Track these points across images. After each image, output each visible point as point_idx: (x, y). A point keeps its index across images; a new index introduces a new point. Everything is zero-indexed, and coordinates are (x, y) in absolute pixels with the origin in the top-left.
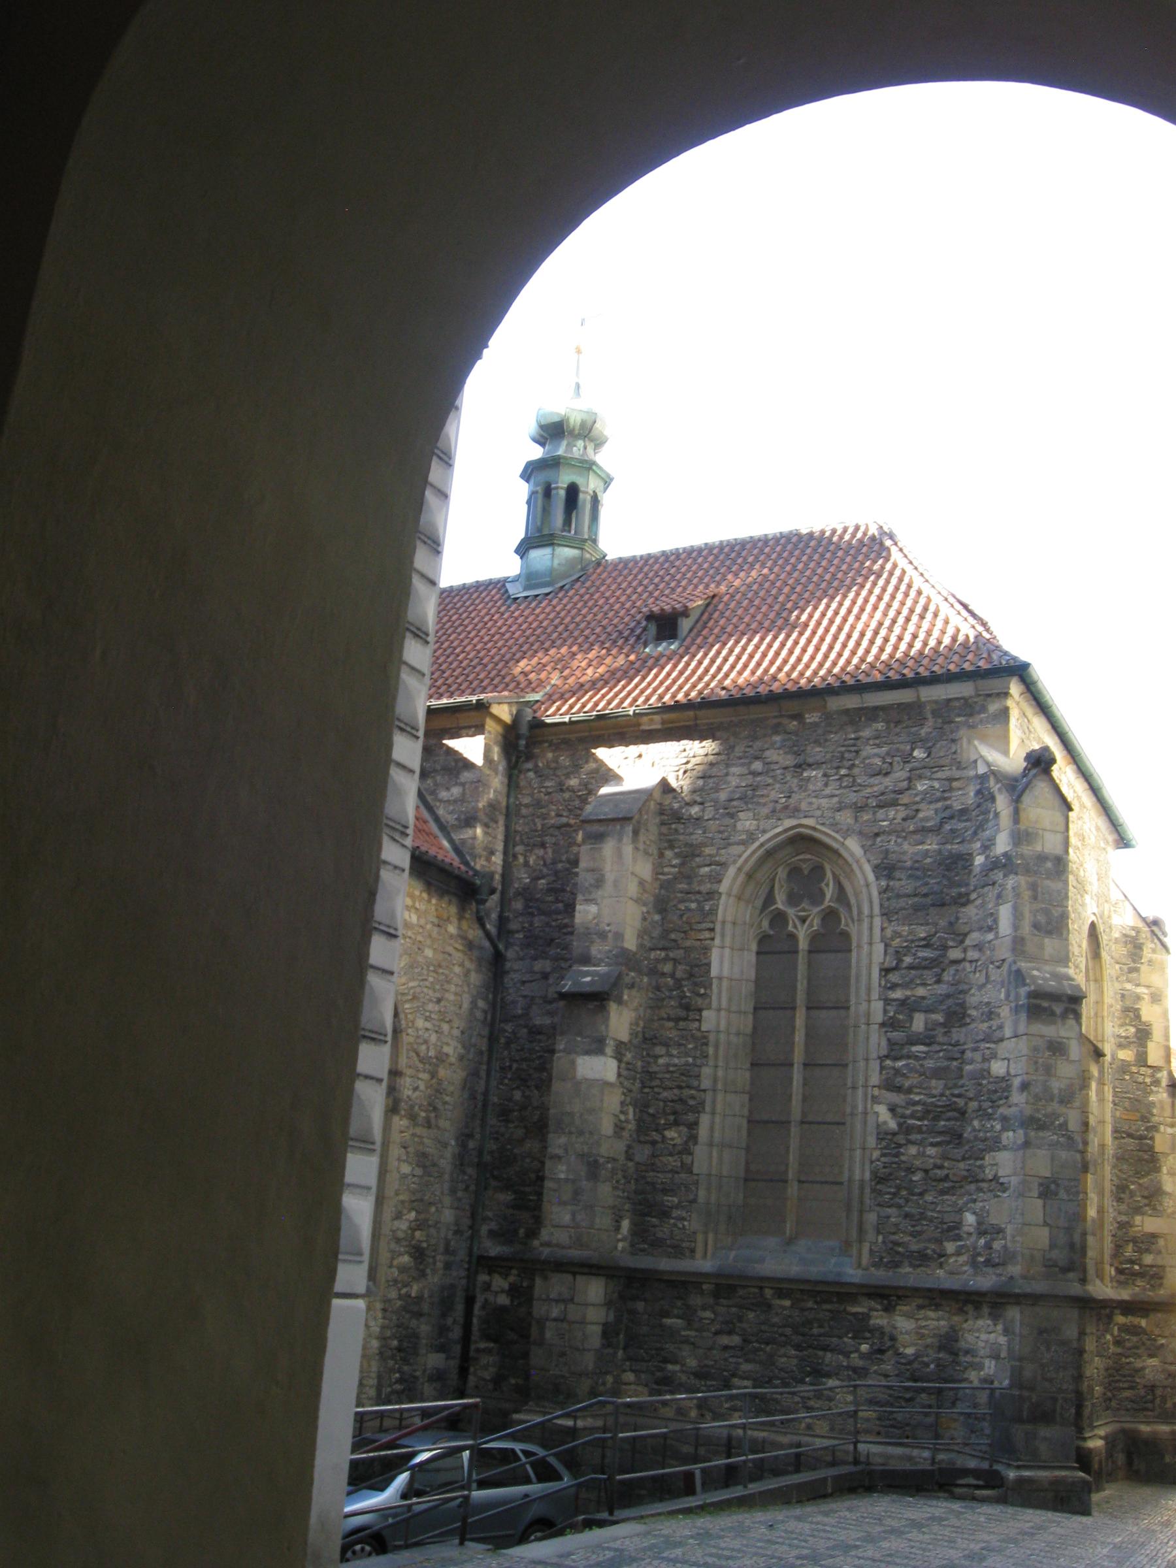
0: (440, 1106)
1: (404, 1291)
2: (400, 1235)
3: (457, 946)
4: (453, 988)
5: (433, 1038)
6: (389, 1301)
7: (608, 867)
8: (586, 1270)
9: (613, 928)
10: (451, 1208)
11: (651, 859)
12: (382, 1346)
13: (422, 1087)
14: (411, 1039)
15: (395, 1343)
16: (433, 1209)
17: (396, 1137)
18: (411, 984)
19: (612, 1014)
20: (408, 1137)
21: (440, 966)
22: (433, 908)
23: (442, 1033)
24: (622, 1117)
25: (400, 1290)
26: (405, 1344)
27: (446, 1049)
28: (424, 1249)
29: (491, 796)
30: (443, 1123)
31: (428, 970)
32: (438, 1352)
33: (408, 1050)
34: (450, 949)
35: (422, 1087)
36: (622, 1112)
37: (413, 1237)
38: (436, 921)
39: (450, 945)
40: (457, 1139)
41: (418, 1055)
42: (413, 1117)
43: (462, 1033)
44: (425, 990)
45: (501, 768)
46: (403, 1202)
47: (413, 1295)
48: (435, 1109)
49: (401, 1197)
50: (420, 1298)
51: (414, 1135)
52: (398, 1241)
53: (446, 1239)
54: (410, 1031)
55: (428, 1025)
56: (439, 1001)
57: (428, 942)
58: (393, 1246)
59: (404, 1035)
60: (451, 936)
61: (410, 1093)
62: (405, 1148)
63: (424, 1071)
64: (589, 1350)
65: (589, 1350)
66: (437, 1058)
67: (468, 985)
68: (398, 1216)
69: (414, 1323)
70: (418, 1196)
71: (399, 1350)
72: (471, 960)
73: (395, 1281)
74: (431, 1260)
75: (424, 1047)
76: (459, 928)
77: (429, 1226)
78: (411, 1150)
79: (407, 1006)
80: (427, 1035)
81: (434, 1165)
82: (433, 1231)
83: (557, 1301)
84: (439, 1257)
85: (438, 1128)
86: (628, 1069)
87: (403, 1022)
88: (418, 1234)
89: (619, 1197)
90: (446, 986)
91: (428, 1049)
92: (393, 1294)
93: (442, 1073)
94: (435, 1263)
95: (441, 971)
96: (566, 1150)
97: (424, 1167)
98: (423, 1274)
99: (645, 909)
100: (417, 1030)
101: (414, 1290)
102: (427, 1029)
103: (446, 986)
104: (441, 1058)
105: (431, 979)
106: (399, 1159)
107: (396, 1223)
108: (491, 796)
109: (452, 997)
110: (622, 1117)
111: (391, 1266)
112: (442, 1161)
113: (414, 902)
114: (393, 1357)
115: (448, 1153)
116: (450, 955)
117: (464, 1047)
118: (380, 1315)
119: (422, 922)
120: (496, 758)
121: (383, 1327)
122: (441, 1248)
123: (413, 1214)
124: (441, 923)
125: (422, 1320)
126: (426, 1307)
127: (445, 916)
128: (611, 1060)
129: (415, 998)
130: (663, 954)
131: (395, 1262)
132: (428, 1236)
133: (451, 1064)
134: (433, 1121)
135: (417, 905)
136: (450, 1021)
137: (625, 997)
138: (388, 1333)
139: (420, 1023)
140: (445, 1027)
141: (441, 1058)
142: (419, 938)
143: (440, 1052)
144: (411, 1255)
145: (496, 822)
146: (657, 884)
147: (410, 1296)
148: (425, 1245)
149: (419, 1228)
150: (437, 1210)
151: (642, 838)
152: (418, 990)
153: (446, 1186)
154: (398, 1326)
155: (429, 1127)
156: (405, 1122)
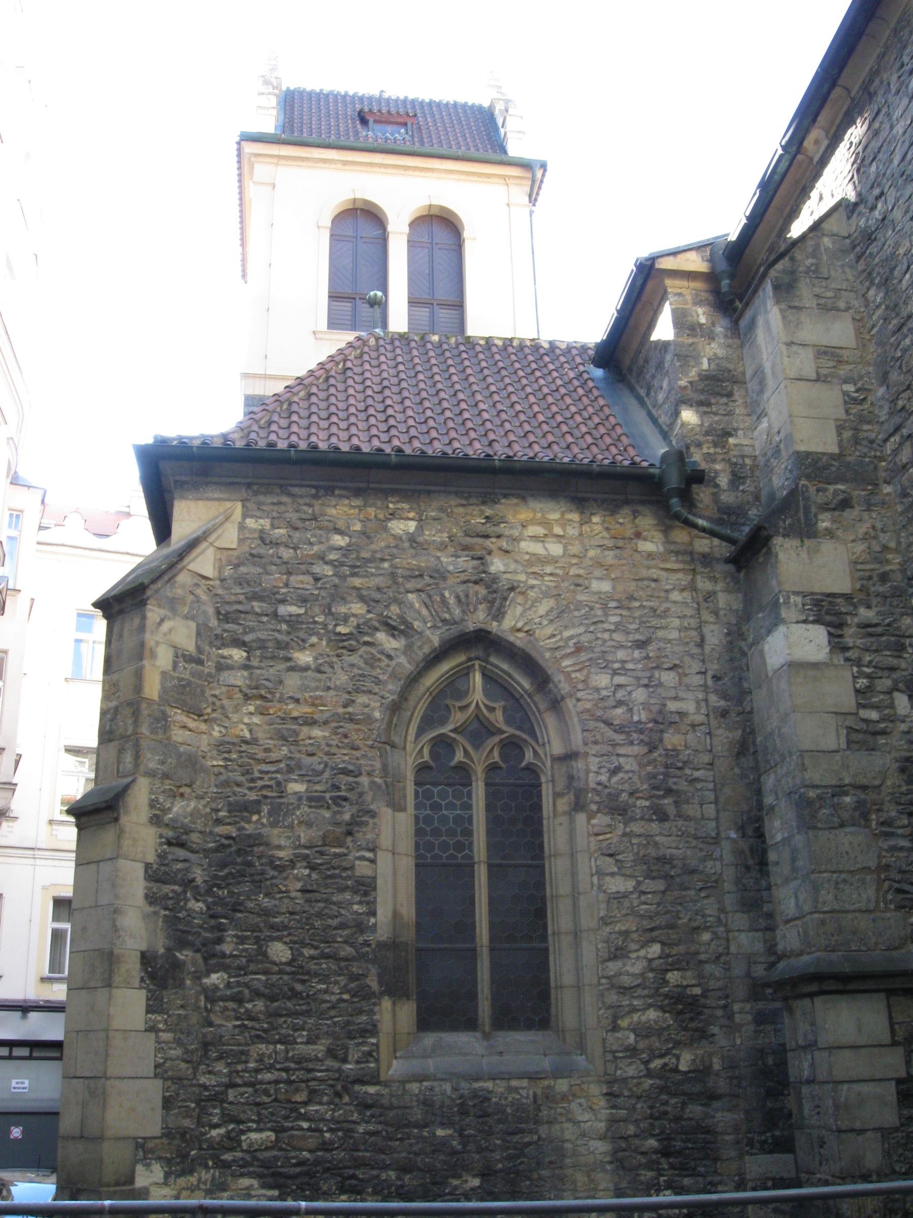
0: (683, 785)
1: (657, 1063)
2: (626, 981)
3: (669, 566)
4: (676, 622)
5: (640, 695)
6: (624, 1080)
7: (765, 356)
8: (814, 987)
9: (782, 434)
10: (752, 929)
11: (847, 316)
12: (615, 1152)
13: (629, 764)
14: (588, 705)
15: (652, 1143)
16: (706, 936)
17: (581, 841)
18: (567, 634)
19: (781, 556)
20: (615, 840)
21: (632, 598)
22: (598, 528)
23: (660, 684)
24: (874, 715)
25: (646, 1063)
26: (678, 1144)
27: (672, 706)
28: (695, 997)
29: (705, 365)
30: (692, 810)
31: (605, 607)
32: (771, 1152)
33: (582, 721)
34: (654, 573)
35: (629, 764)
36: (860, 706)
37: (666, 982)
38: (610, 543)
39: (649, 568)
40: (741, 829)
41: (608, 724)
42: (617, 809)
43: (716, 678)
44: (606, 636)
45: (719, 329)
46: (626, 934)
47: (683, 1067)
48: (669, 791)
49: (618, 927)
50: (702, 1072)
51: (625, 834)
52: (624, 990)
53: (748, 975)
54: (580, 695)
55: (619, 680)
56: (641, 645)
57: (598, 573)
58: (612, 997)
59: (570, 703)
60: (650, 555)
61: (603, 778)
62: (611, 855)
63: (632, 743)
64: (861, 1132)
65: (861, 1132)
66: (656, 722)
67: (716, 613)
68: (618, 954)
69: (695, 1110)
70: (660, 921)
71: (666, 1153)
72: (714, 579)
73: (632, 1051)
74: (719, 1013)
75: (619, 711)
76: (668, 542)
77: (701, 962)
78: (627, 857)
79: (565, 663)
80: (620, 694)
81: (694, 871)
82: (709, 968)
83: (805, 1048)
84: (736, 1007)
85: (688, 818)
86: (871, 635)
87: (561, 685)
88: (673, 977)
89: (893, 849)
90: (655, 622)
91: (630, 710)
92: (631, 1070)
93: (672, 739)
94: (731, 1017)
95: (637, 604)
96: (776, 794)
97: (667, 877)
98: (703, 1035)
99: (850, 388)
100: (597, 690)
101: (685, 1060)
102: (620, 686)
103: (655, 622)
104: (663, 720)
105: (613, 619)
106: (600, 873)
107: (613, 967)
108: (705, 365)
109: (674, 635)
110: (874, 715)
111: (615, 1028)
112: (709, 864)
113: (551, 529)
114: (649, 1166)
115: (726, 851)
116: (655, 580)
117: (724, 696)
118: (602, 1103)
119: (575, 549)
120: (703, 320)
121: (612, 1121)
122: (740, 990)
123: (655, 949)
124: (619, 543)
125: (716, 1104)
126: (722, 1086)
127: (629, 533)
128: (795, 627)
129: (579, 649)
130: (897, 438)
131: (624, 1023)
132: (700, 976)
133: (693, 726)
134: (671, 811)
135: (558, 530)
136: (674, 668)
137: (824, 523)
138: (631, 1129)
139: (602, 680)
140: (668, 678)
141: (663, 720)
142: (573, 571)
143: (660, 712)
144: (663, 1009)
145: (730, 395)
146: (872, 347)
147: (676, 1070)
148: (697, 991)
149: (675, 966)
150: (716, 936)
151: (806, 292)
152: (585, 638)
153: (730, 900)
154: (651, 1116)
155: (662, 817)
156: (601, 820)
